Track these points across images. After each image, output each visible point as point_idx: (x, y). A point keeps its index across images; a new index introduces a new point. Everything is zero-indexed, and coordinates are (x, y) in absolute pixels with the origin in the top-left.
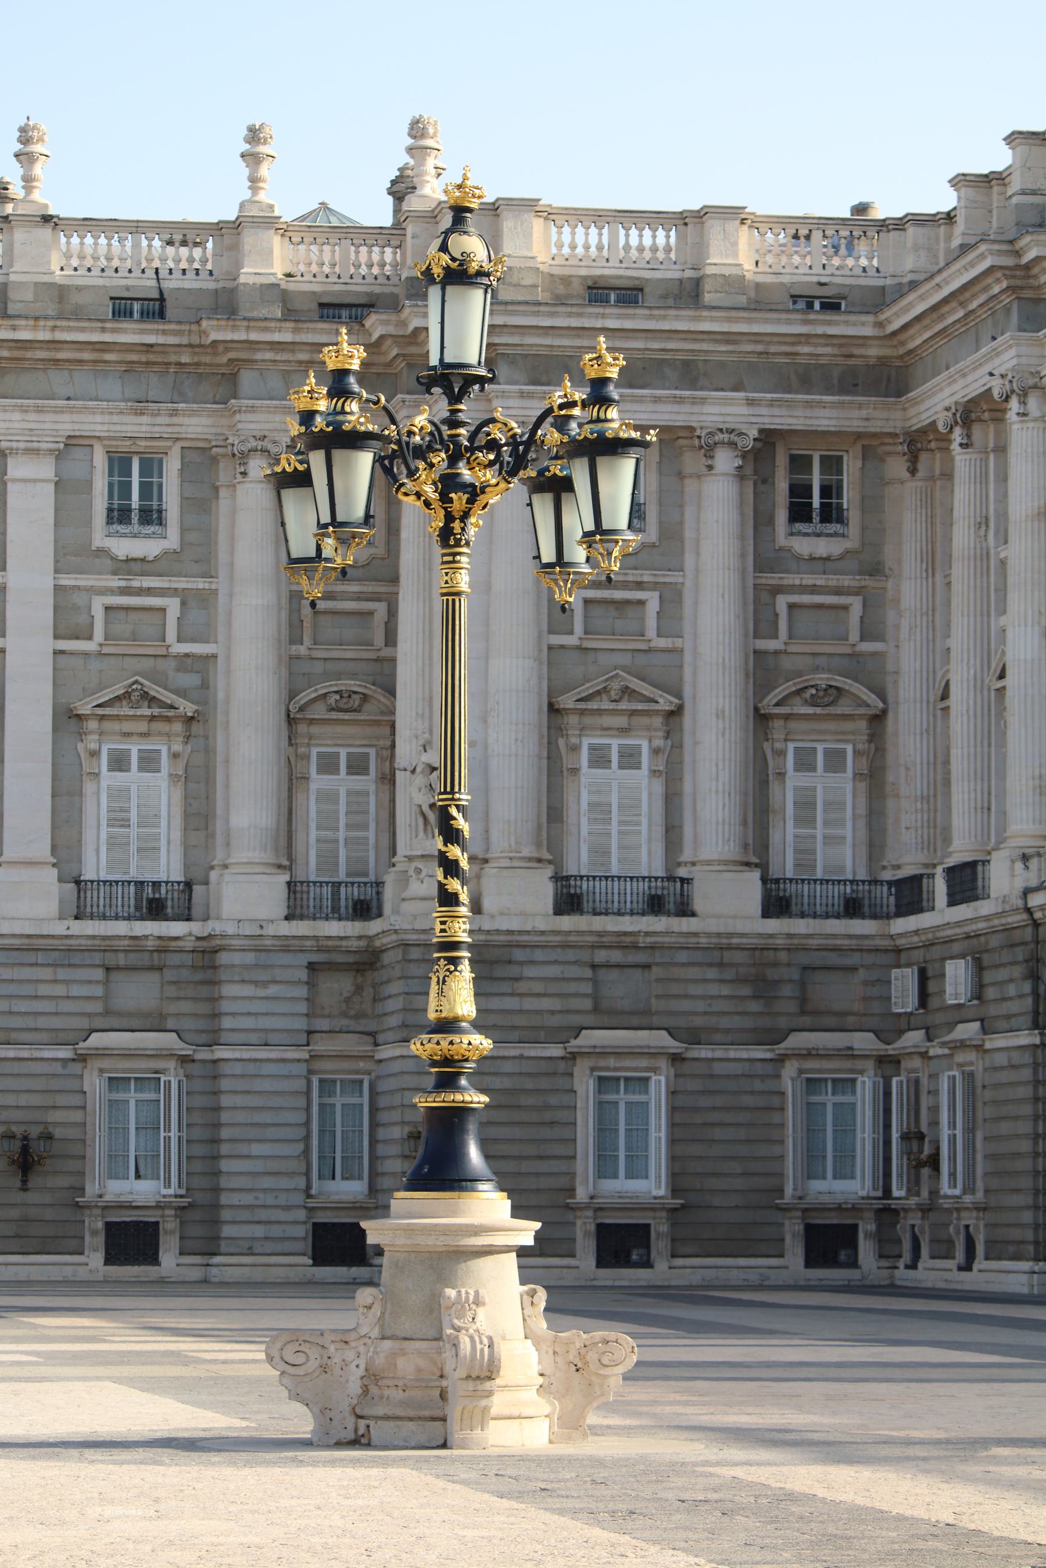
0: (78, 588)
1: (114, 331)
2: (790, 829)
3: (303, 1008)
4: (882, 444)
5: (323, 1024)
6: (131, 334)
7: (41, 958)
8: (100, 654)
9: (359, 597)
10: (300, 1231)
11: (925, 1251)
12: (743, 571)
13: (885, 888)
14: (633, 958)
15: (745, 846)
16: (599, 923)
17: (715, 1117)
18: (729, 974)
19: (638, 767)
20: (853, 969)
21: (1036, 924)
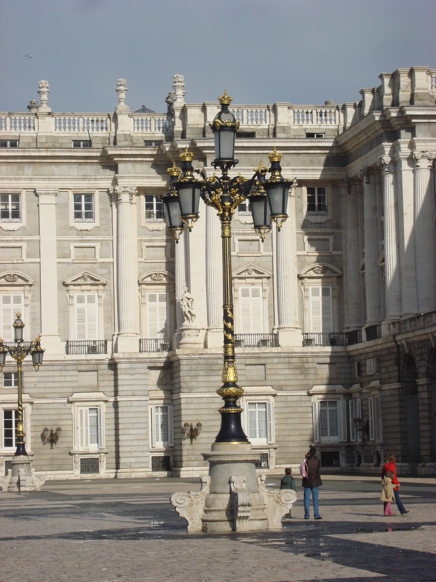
0: (65, 240)
1: (74, 151)
2: (311, 316)
4: (339, 183)
7: (56, 368)
11: (363, 460)
13: (344, 335)
14: (258, 361)
16: (248, 350)
18: (292, 366)
19: (258, 296)
21: (398, 346)
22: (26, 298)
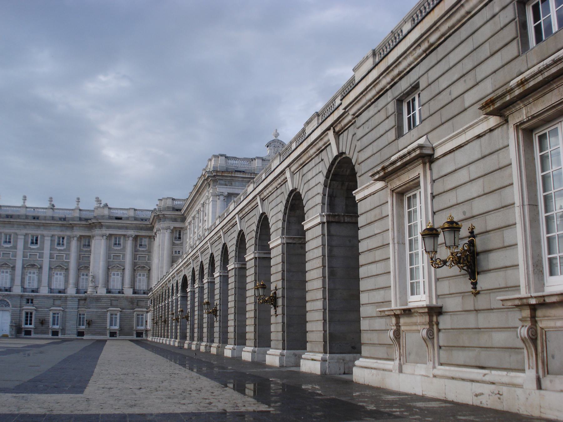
3: (77, 305)
5: (80, 307)
6: (60, 222)
8: (55, 261)
9: (88, 255)
10: (76, 332)
12: (133, 252)
15: (131, 286)
17: (125, 319)
18: (128, 301)
20: (144, 301)
22: (37, 273)
